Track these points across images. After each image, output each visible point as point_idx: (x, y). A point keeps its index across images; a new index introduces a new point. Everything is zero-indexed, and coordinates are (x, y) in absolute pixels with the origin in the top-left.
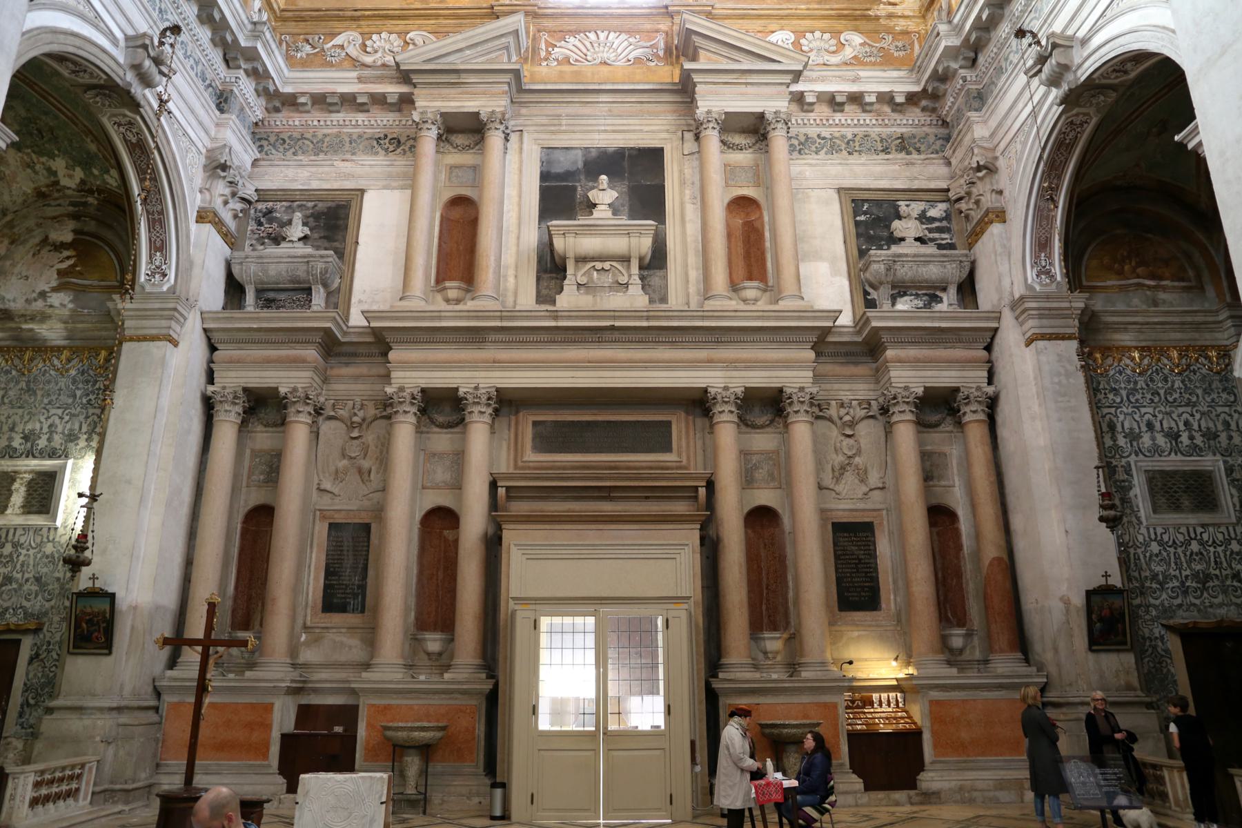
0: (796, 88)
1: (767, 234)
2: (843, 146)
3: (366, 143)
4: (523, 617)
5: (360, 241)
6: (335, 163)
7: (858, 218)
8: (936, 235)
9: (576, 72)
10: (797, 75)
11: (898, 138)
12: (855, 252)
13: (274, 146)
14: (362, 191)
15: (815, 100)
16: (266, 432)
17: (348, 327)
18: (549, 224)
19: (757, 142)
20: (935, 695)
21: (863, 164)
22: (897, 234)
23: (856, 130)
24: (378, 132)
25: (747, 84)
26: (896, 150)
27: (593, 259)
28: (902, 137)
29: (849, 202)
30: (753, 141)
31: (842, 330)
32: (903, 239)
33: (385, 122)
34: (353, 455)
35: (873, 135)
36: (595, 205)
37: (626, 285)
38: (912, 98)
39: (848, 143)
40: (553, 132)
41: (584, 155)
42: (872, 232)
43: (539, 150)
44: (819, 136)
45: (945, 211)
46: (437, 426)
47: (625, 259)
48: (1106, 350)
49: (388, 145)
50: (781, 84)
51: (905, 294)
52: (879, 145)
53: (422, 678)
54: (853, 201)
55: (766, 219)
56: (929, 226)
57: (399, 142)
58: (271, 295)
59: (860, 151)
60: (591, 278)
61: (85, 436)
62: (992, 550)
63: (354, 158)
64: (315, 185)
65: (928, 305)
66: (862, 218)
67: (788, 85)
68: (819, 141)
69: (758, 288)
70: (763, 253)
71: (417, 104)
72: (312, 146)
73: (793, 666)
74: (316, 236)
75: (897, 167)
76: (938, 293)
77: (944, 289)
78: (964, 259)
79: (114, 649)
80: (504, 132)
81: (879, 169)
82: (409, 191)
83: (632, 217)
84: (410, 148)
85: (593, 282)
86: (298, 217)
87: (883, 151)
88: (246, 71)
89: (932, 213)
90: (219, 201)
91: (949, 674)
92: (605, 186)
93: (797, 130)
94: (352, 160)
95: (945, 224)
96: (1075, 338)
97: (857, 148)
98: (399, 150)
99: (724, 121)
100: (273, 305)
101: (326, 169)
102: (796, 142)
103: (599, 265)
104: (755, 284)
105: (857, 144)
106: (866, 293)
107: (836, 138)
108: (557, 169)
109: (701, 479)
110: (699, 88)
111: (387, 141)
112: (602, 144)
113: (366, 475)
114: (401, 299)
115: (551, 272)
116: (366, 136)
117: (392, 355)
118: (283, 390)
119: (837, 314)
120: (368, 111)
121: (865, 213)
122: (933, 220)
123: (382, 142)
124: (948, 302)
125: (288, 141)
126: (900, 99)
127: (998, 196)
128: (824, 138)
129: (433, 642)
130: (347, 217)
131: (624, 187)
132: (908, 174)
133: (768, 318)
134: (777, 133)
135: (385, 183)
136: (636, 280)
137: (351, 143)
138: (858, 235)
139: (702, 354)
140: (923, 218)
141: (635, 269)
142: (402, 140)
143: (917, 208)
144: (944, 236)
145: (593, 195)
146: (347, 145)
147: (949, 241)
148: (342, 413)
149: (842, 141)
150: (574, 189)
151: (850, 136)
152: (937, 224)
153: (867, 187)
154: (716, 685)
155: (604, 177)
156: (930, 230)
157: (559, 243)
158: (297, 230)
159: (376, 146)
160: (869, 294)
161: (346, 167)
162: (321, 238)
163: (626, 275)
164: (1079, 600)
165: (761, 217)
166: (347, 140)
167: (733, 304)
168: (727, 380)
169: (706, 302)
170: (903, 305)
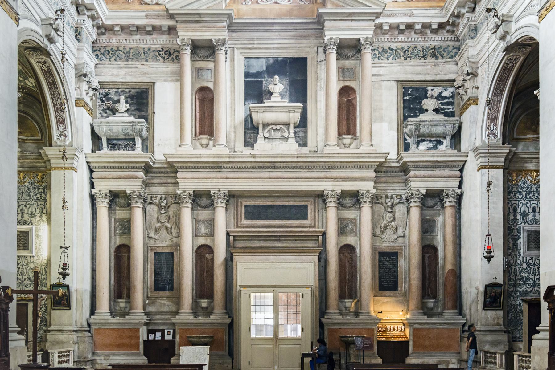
0: (378, 21)
1: (358, 108)
2: (402, 54)
3: (152, 54)
4: (244, 292)
5: (155, 112)
6: (138, 66)
7: (405, 98)
8: (445, 107)
9: (261, 9)
10: (378, 15)
11: (432, 49)
12: (402, 117)
13: (104, 55)
14: (154, 83)
15: (388, 28)
16: (121, 210)
17: (155, 160)
18: (250, 106)
19: (356, 53)
20: (416, 326)
21: (411, 66)
22: (425, 107)
23: (410, 44)
24: (158, 47)
25: (352, 20)
26: (430, 56)
27: (271, 124)
28: (434, 48)
29: (401, 89)
30: (354, 53)
31: (390, 161)
32: (427, 110)
33: (162, 41)
34: (163, 221)
35: (419, 47)
36: (271, 94)
37: (287, 138)
38: (441, 26)
39: (405, 52)
40: (250, 48)
41: (266, 62)
42: (412, 106)
43: (243, 59)
44: (389, 48)
45: (452, 93)
46: (201, 207)
47: (287, 125)
48: (519, 172)
49: (164, 55)
50: (370, 20)
51: (424, 140)
52: (422, 53)
53: (200, 318)
54: (404, 88)
55: (358, 99)
56: (442, 102)
57: (170, 53)
58: (115, 142)
59: (411, 57)
60: (270, 135)
61: (39, 215)
62: (449, 266)
63: (147, 63)
64: (128, 79)
65: (435, 147)
66: (408, 98)
67: (374, 20)
68: (389, 51)
69: (352, 138)
70: (355, 118)
71: (179, 34)
72: (124, 55)
73: (357, 314)
74: (133, 108)
75: (429, 67)
76: (441, 140)
77: (445, 138)
78: (456, 122)
79: (71, 307)
80: (225, 51)
81: (419, 68)
82: (179, 83)
83: (291, 101)
84: (176, 57)
85: (272, 136)
86: (122, 98)
87: (423, 57)
88: (88, 17)
89: (446, 94)
90: (84, 93)
91: (424, 318)
92: (277, 82)
93: (378, 44)
94: (147, 65)
95: (451, 100)
96: (502, 168)
97: (409, 56)
98: (170, 58)
99: (339, 44)
100: (116, 147)
101: (134, 70)
102: (376, 52)
103: (274, 127)
104: (350, 136)
105: (410, 53)
106: (405, 139)
107: (399, 49)
108: (253, 71)
109: (320, 232)
110: (326, 24)
111: (163, 52)
112: (276, 56)
113: (169, 230)
114: (180, 146)
115: (251, 129)
116: (152, 49)
117: (179, 175)
118: (128, 192)
119: (387, 155)
120: (152, 35)
121: (409, 95)
122: (445, 98)
123: (161, 53)
124: (445, 147)
125: (111, 52)
126: (435, 27)
127: (476, 90)
128: (392, 49)
129: (204, 303)
130: (147, 98)
131: (286, 82)
132: (435, 71)
133: (354, 157)
134: (366, 51)
135: (165, 78)
136: (292, 135)
137: (144, 54)
138: (404, 108)
139: (322, 174)
140: (440, 97)
141: (292, 129)
142: (172, 51)
143: (437, 91)
144: (449, 107)
145: (271, 87)
146: (143, 54)
147: (451, 110)
148: (156, 201)
149: (402, 51)
150: (261, 82)
151: (406, 48)
152: (447, 100)
153: (412, 79)
154: (323, 320)
155: (277, 77)
156: (442, 104)
157: (254, 116)
158: (123, 106)
159: (158, 56)
160: (406, 140)
161: (144, 69)
162: (135, 110)
163: (287, 132)
164: (482, 289)
165: (355, 98)
166: (142, 51)
167: (337, 150)
168: (334, 187)
169: (325, 148)
170: (423, 146)
